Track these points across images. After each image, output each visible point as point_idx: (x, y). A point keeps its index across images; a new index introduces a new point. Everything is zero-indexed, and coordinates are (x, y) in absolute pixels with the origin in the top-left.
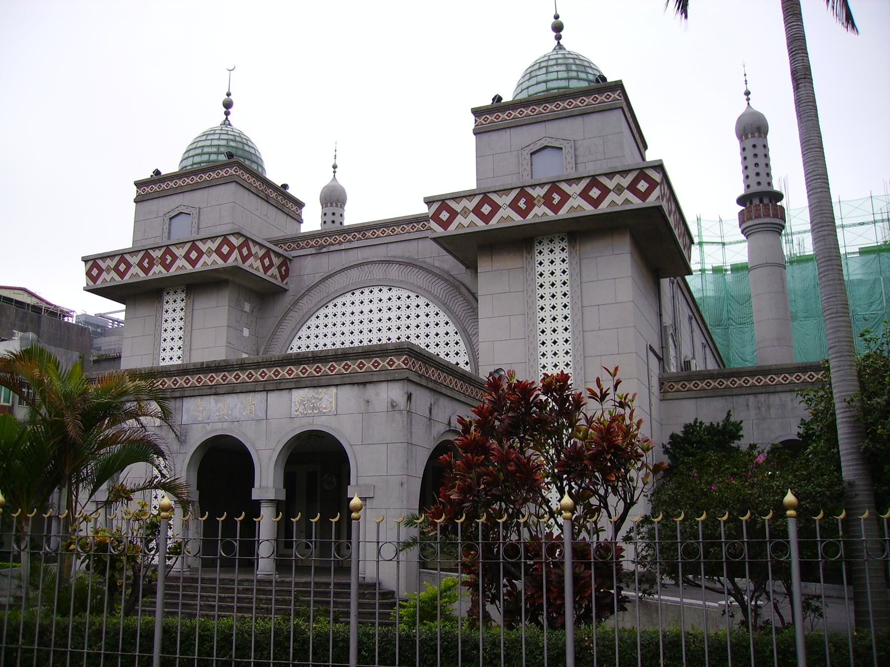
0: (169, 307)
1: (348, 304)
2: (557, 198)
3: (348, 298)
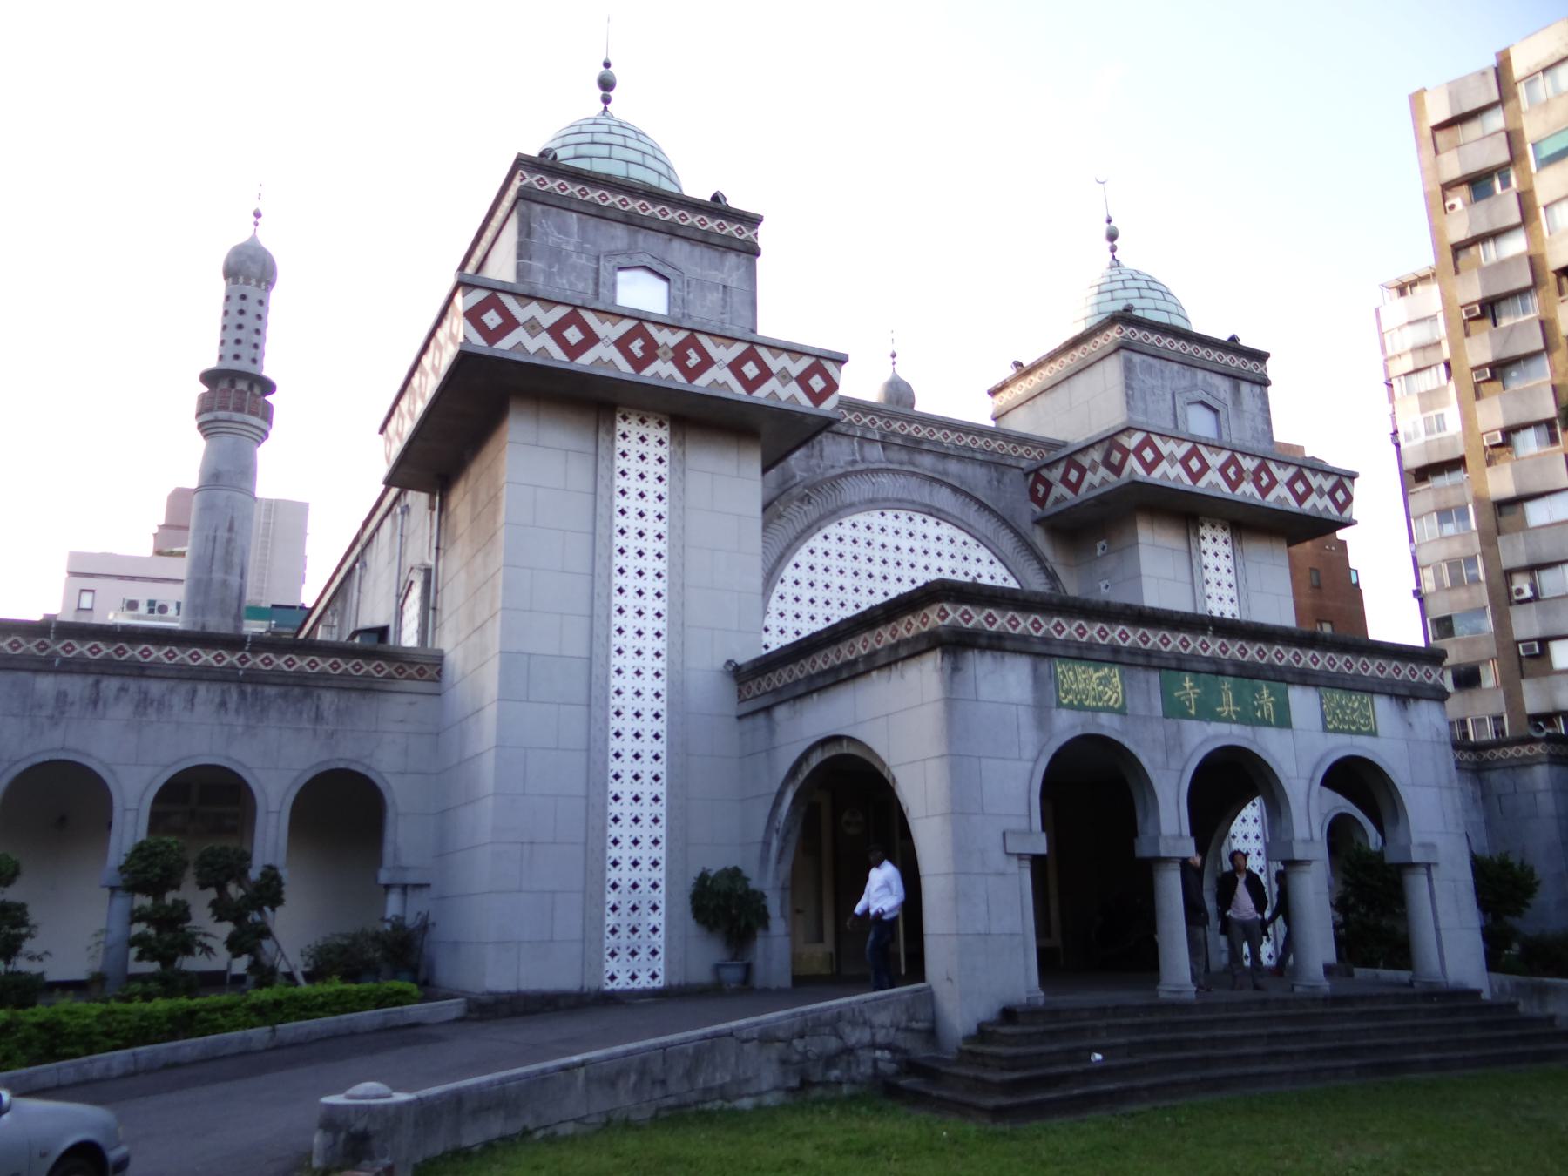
0: (632, 446)
1: (876, 528)
3: (874, 518)
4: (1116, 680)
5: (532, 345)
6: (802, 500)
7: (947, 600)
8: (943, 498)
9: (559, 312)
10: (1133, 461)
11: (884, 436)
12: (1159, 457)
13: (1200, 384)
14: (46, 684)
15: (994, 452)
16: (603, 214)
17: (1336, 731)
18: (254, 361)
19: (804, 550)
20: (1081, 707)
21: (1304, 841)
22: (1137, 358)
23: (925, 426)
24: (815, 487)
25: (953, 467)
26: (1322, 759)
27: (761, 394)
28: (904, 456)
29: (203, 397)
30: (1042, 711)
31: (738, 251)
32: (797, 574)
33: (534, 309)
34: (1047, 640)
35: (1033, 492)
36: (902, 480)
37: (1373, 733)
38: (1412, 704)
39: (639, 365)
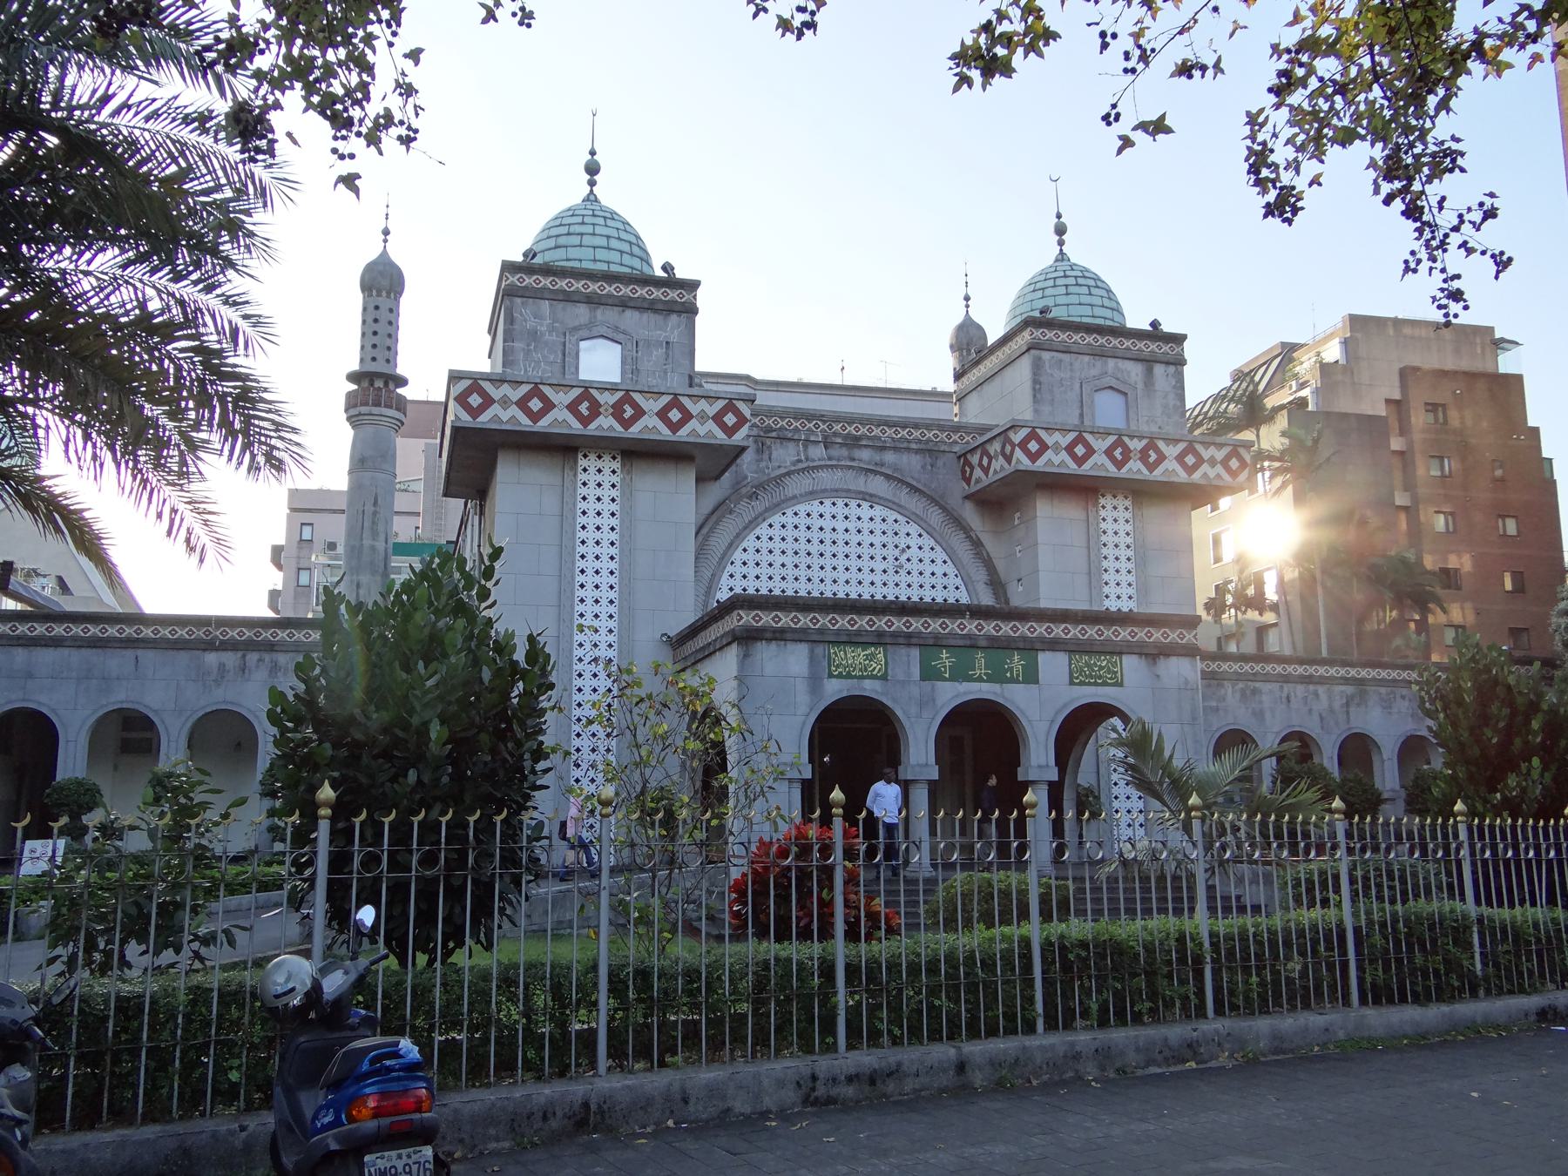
1: (815, 515)
2: (1153, 456)
3: (815, 507)
4: (881, 656)
5: (505, 416)
6: (750, 498)
7: (742, 608)
8: (878, 485)
9: (525, 389)
10: (1018, 453)
11: (825, 437)
12: (1044, 447)
13: (1110, 371)
14: (211, 658)
15: (929, 440)
16: (568, 298)
17: (1082, 683)
18: (388, 361)
19: (752, 537)
20: (849, 676)
21: (1040, 767)
22: (1046, 355)
23: (863, 425)
24: (761, 486)
25: (889, 457)
26: (1065, 705)
27: (683, 433)
28: (844, 452)
29: (349, 395)
30: (814, 683)
31: (679, 312)
32: (745, 557)
33: (506, 389)
34: (821, 631)
35: (963, 472)
36: (839, 473)
37: (1120, 684)
38: (1162, 662)
39: (585, 421)
